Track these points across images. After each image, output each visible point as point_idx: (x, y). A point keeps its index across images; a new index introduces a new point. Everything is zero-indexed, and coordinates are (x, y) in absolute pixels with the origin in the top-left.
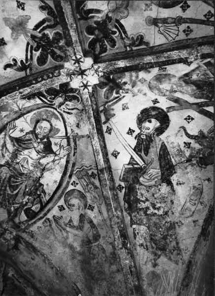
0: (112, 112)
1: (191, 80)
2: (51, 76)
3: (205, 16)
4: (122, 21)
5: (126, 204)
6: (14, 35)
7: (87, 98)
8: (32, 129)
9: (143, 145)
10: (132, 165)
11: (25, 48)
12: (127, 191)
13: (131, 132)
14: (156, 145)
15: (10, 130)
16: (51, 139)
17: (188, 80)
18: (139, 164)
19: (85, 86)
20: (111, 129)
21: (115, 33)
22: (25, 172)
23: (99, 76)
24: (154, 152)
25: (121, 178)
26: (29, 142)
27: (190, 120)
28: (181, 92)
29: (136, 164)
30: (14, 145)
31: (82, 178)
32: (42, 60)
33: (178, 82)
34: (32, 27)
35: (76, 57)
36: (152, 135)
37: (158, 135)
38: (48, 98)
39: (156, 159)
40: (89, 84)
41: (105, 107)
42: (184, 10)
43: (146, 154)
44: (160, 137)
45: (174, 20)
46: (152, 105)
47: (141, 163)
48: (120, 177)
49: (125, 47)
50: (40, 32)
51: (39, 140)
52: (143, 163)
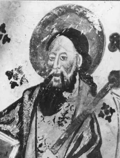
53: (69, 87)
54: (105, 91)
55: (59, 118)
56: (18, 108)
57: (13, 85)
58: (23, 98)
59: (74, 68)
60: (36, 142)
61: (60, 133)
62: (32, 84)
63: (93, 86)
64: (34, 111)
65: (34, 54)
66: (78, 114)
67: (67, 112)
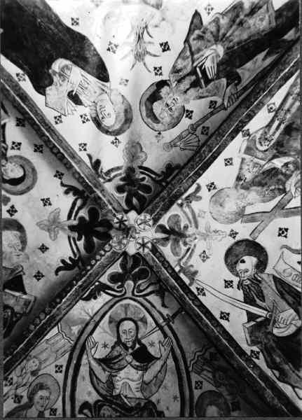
0: (193, 270)
1: (248, 182)
2: (103, 252)
4: (145, 165)
5: (275, 372)
6: (52, 235)
7: (153, 258)
8: (115, 340)
9: (252, 293)
10: (254, 321)
11: (68, 243)
12: (265, 353)
13: (228, 284)
14: (267, 283)
15: (91, 349)
16: (143, 341)
17: (245, 184)
18: (260, 316)
19: (144, 245)
20: (203, 290)
22: (133, 404)
24: (270, 291)
25: (249, 342)
26: (120, 358)
27: (285, 233)
29: (257, 318)
30: (104, 370)
31: (203, 370)
32: (89, 246)
34: (66, 218)
35: (118, 219)
36: (256, 275)
37: (262, 271)
38: (116, 288)
39: (278, 299)
40: (146, 241)
41: (181, 266)
42: (190, 118)
43: (264, 301)
44: (266, 271)
46: (231, 241)
47: (263, 313)
48: (247, 341)
49: (161, 185)
50: (75, 219)
51: (130, 351)
52: (266, 312)
57: (14, 143)
58: (5, 144)
62: (9, 149)
65: (21, 158)
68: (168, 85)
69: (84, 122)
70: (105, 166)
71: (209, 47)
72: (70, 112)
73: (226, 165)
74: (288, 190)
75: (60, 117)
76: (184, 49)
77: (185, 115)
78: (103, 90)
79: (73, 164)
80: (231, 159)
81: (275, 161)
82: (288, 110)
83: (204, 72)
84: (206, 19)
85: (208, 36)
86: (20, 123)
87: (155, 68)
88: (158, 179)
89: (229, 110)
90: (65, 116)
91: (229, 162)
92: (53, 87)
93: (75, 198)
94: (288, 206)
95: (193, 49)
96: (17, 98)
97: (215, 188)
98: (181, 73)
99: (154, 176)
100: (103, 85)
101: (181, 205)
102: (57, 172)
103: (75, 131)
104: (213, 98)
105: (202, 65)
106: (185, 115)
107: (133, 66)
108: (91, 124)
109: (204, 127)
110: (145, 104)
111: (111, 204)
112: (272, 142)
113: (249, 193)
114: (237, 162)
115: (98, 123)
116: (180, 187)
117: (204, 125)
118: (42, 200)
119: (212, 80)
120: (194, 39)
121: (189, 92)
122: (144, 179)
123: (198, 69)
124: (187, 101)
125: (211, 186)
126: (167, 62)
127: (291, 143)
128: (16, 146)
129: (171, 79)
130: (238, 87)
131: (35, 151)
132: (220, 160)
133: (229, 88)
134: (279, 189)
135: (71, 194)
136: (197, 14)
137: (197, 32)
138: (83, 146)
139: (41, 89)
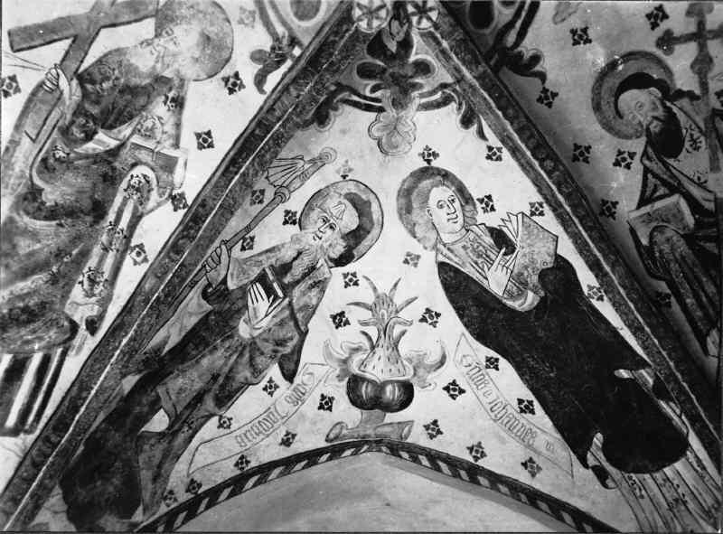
1: (159, 95)
3: (252, 239)
4: (373, 115)
21: (374, 90)
23: (359, 5)
28: (148, 43)
33: (176, 66)
35: (429, 19)
42: (287, 212)
45: (292, 189)
53: (670, 118)
54: (704, 85)
55: (691, 146)
56: (650, 176)
57: (628, 167)
59: (658, 103)
60: (692, 180)
61: (703, 155)
62: (642, 149)
63: (691, 96)
64: (665, 164)
65: (618, 134)
66: (702, 125)
67: (692, 135)
68: (331, 260)
69: (489, 197)
70: (451, 114)
71: (265, 331)
72: (513, 218)
73: (209, 133)
74: (75, 82)
75: (533, 214)
76: (308, 322)
77: (298, 216)
78: (449, 249)
79: (516, 136)
80: (201, 147)
81: (113, 143)
82: (106, 249)
83: (269, 291)
84: (274, 372)
85: (268, 348)
86: (609, 208)
87: (356, 284)
88: (345, 95)
89: (217, 243)
90: (523, 214)
91: (205, 141)
92: (540, 266)
93: (519, 49)
94: (65, 44)
95: (292, 323)
96: (607, 268)
97: (226, 80)
98: (310, 282)
99: (355, 98)
100: (448, 258)
101: (294, 41)
102: (550, 105)
103: (510, 189)
104: (248, 254)
105: (274, 301)
106: (298, 216)
107: (396, 285)
108: (476, 194)
109: (261, 202)
110: (373, 225)
111: (443, 52)
112: (124, 185)
113: (154, 68)
114: (188, 140)
115: (461, 190)
116: (298, 97)
117: (259, 207)
118: (590, 41)
119: (253, 282)
120: (291, 339)
121: (295, 255)
122: (374, 90)
123: (280, 293)
124: (295, 239)
125: (233, 84)
126: (336, 296)
127: (87, 185)
128: (624, 159)
129: (326, 270)
130: (206, 282)
131: (588, 149)
132: (224, 142)
133: (222, 277)
134: (93, 82)
135: (527, 56)
136: (290, 376)
137: (287, 350)
138: (492, 155)
139: (562, 265)
